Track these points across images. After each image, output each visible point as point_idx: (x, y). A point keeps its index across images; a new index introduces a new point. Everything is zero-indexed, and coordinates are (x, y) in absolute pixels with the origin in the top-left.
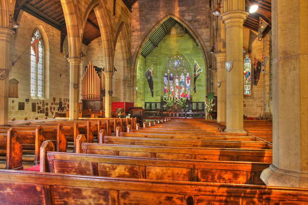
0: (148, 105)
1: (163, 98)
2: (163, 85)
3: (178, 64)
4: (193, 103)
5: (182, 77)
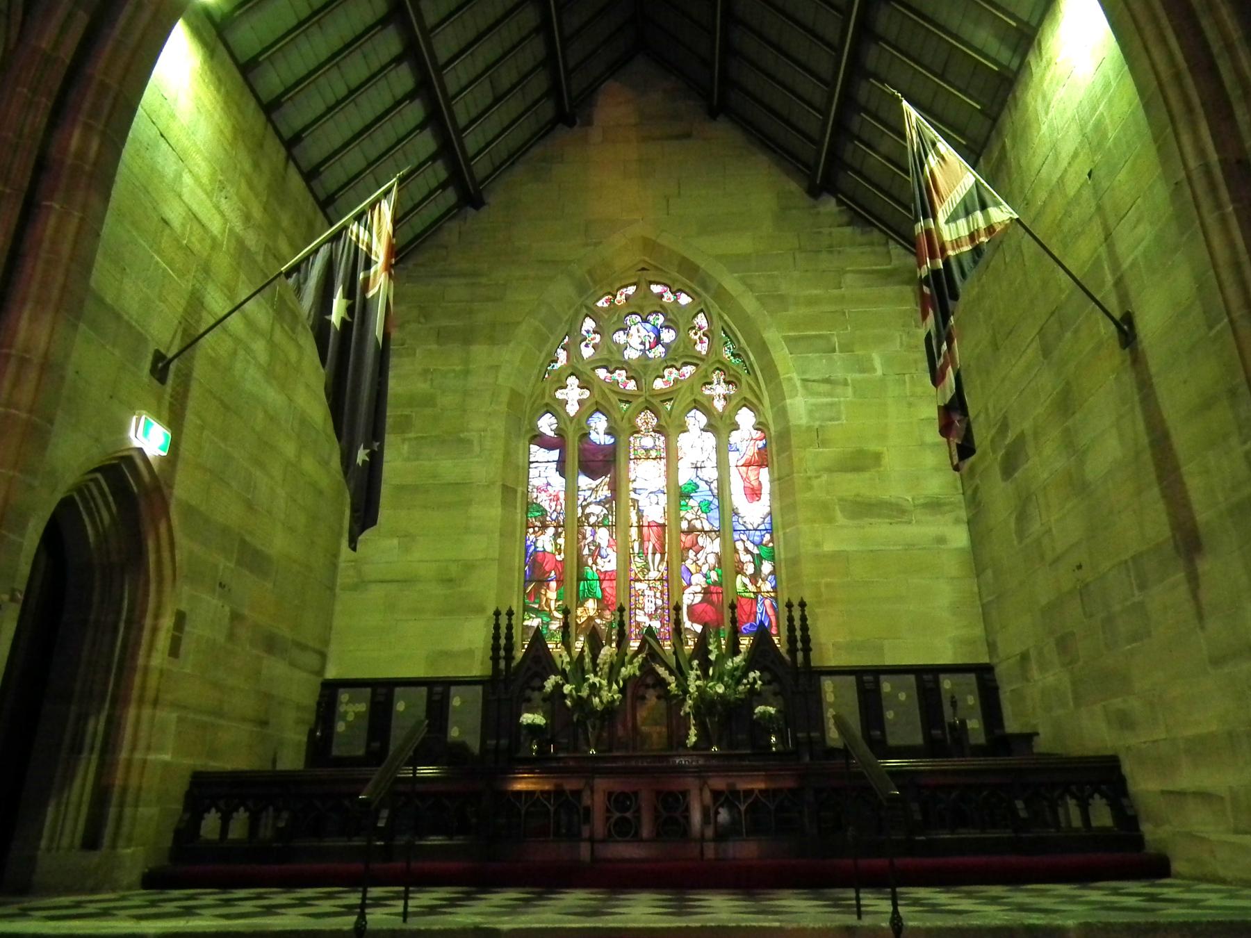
0: (352, 708)
1: (509, 637)
2: (519, 516)
3: (658, 341)
4: (828, 684)
5: (695, 443)
